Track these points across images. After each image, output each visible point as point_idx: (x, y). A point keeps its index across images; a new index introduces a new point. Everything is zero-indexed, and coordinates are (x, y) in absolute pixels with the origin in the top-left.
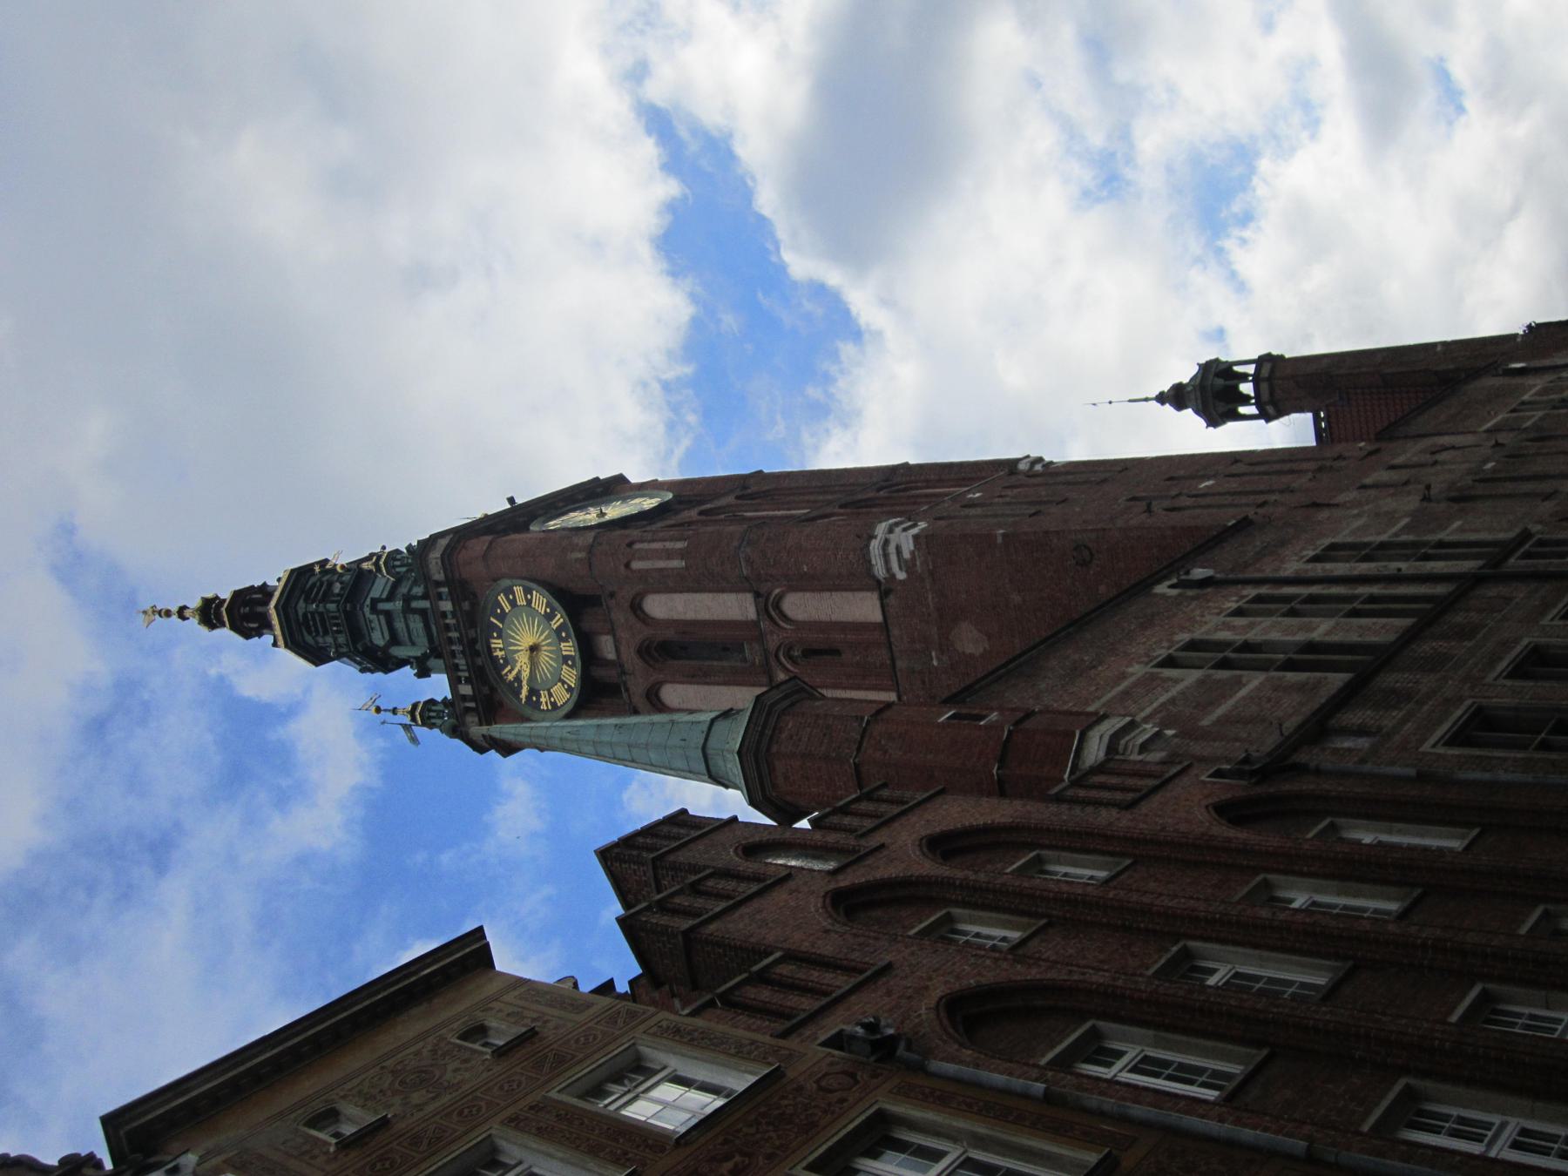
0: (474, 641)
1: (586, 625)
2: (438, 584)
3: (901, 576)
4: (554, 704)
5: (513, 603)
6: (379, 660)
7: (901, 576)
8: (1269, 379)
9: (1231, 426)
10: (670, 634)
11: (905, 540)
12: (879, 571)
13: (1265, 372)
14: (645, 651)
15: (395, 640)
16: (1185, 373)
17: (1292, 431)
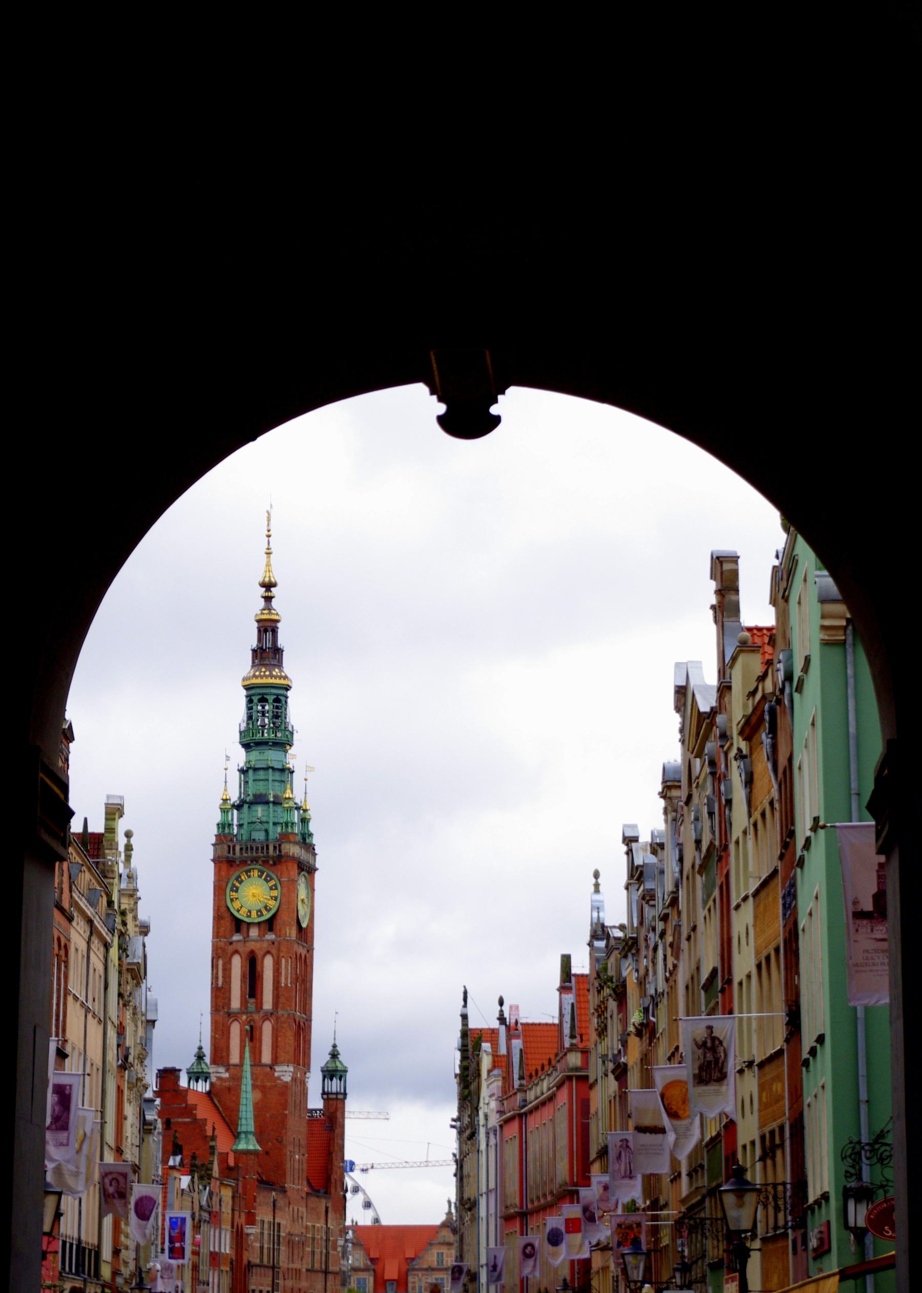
0: (257, 861)
1: (262, 926)
2: (280, 845)
3: (276, 1074)
4: (232, 900)
5: (271, 888)
6: (246, 746)
7: (276, 1074)
8: (337, 1099)
9: (320, 1076)
10: (259, 968)
11: (287, 1078)
12: (277, 1068)
13: (340, 1097)
14: (252, 952)
15: (256, 770)
16: (344, 1059)
17: (315, 1102)
